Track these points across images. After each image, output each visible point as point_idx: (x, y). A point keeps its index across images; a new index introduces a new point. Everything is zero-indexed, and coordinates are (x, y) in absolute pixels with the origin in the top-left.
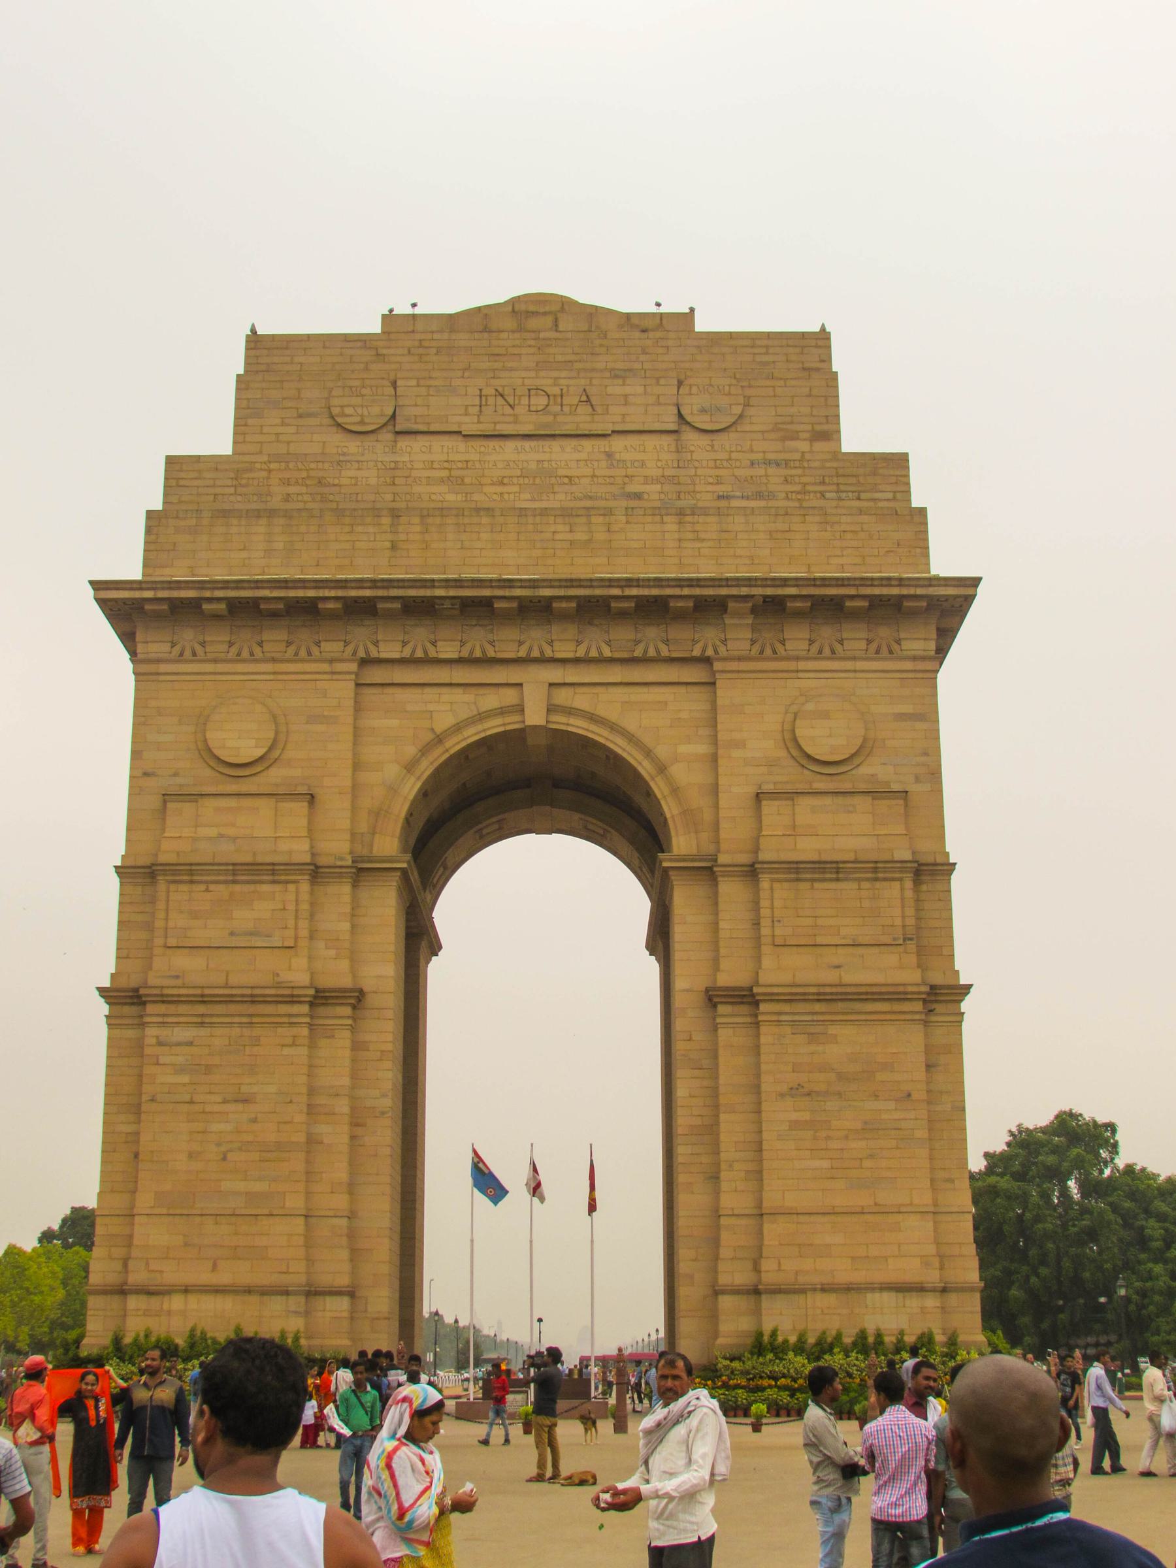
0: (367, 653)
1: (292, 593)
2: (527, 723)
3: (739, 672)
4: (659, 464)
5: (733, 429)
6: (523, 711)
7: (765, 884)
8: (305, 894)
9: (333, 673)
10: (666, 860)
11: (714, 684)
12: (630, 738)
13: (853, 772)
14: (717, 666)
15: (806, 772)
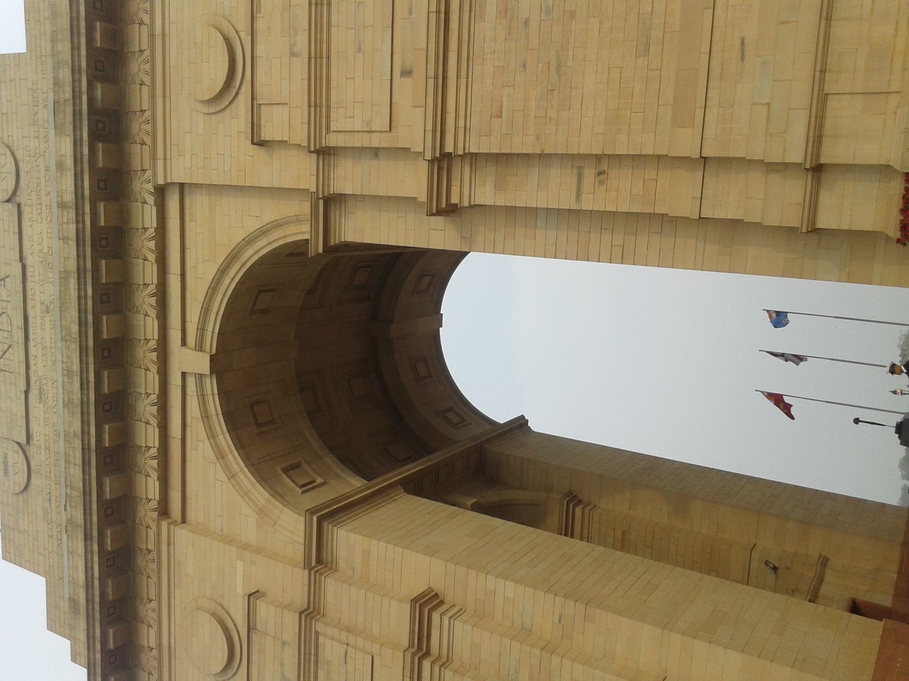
0: (154, 510)
1: (96, 574)
2: (207, 371)
3: (165, 159)
4: (39, 221)
5: (16, 152)
6: (201, 375)
7: (333, 140)
8: (329, 631)
9: (169, 545)
10: (317, 248)
11: (182, 186)
12: (223, 271)
13: (242, 34)
14: (161, 182)
15: (243, 90)
